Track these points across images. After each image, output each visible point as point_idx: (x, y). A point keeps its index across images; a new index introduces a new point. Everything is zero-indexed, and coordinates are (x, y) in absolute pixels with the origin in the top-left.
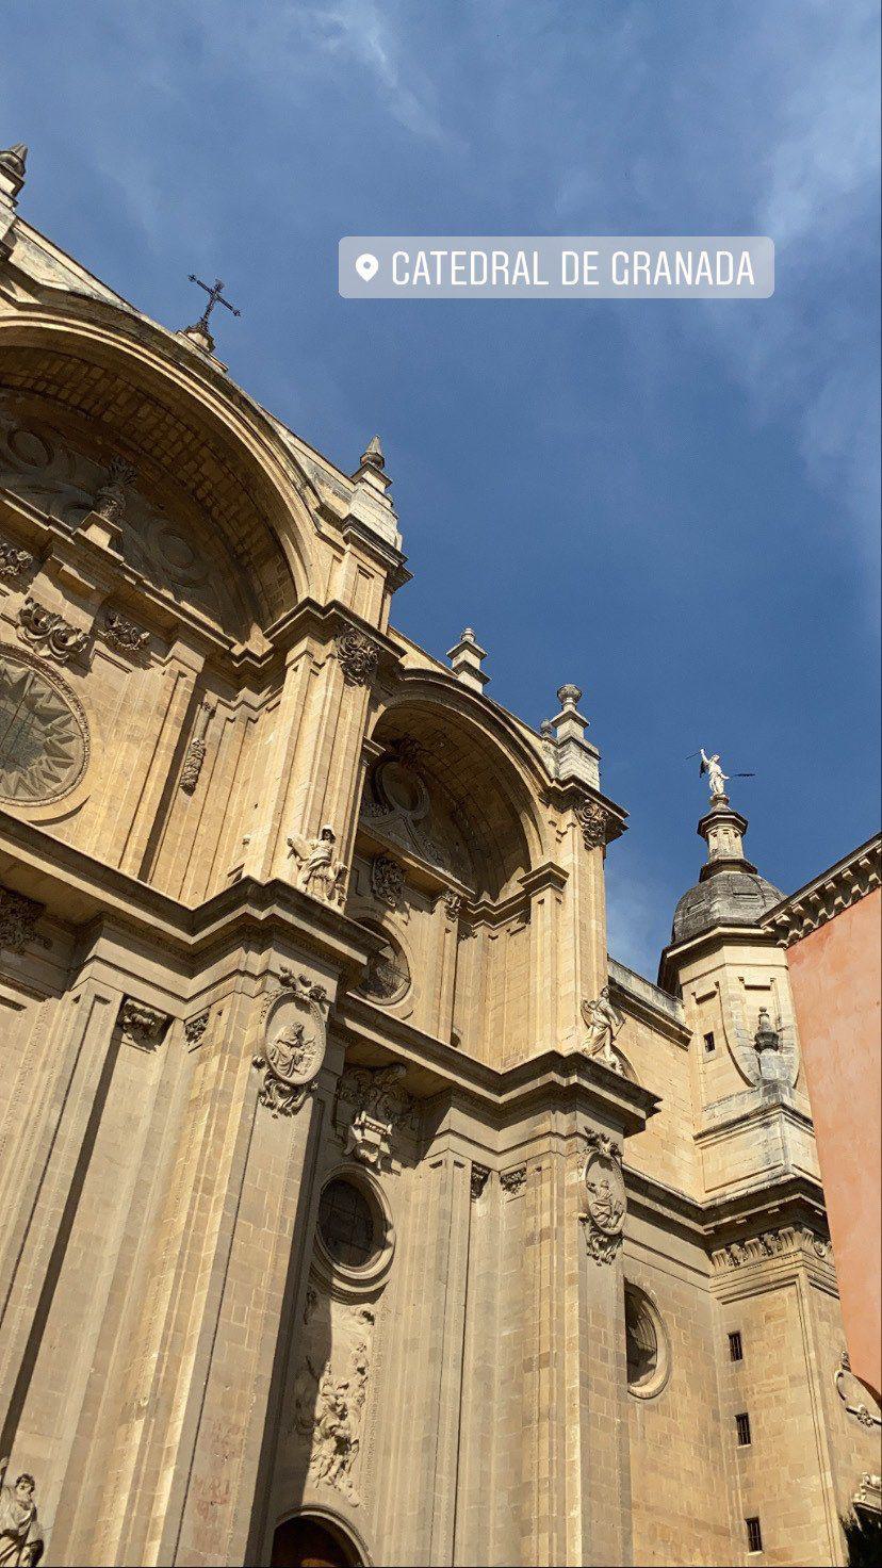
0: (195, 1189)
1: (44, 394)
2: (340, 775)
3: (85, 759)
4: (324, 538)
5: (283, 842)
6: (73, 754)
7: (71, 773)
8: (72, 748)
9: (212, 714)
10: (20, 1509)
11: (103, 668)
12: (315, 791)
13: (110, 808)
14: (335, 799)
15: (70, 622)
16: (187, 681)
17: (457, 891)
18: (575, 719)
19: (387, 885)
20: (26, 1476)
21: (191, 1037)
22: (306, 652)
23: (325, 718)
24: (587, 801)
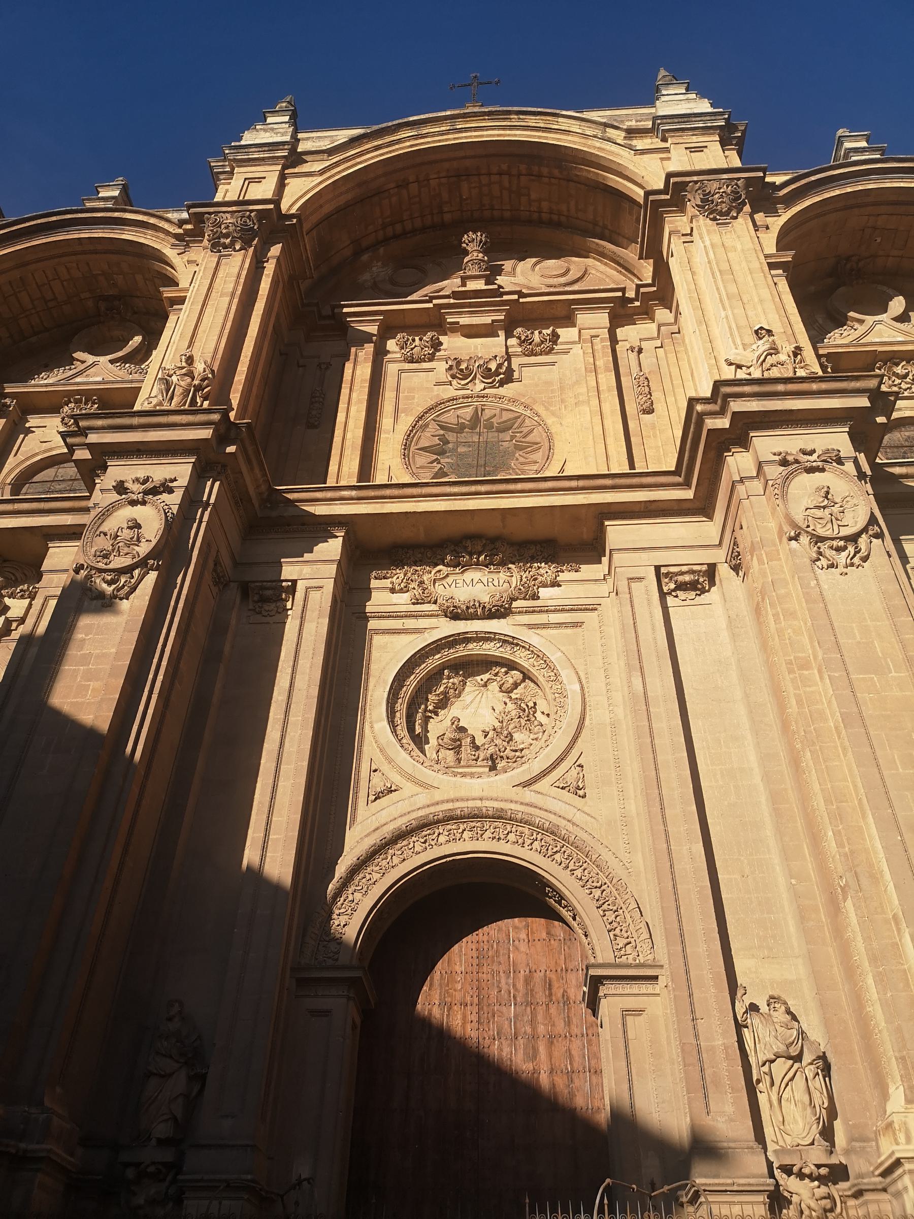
0: (791, 671)
1: (396, 237)
4: (643, 152)
6: (538, 440)
7: (543, 452)
10: (780, 1030)
12: (733, 314)
13: (586, 458)
14: (760, 309)
15: (487, 357)
19: (897, 381)
20: (772, 997)
21: (736, 568)
22: (670, 235)
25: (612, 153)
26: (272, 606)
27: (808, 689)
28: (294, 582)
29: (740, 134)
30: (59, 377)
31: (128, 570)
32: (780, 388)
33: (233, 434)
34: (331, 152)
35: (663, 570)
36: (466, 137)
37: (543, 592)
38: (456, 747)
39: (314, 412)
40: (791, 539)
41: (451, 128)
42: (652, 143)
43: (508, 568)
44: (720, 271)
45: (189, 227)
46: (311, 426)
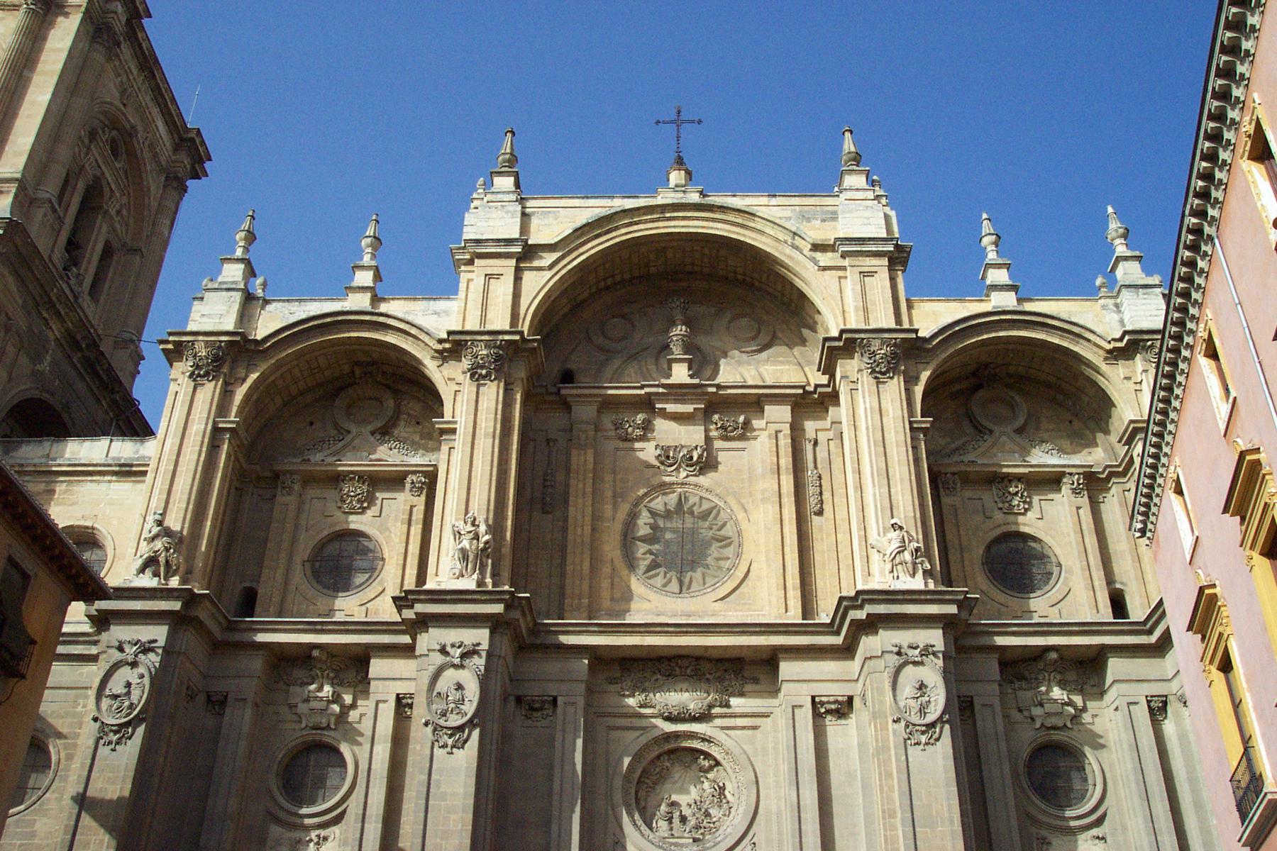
0: (884, 818)
1: (607, 288)
2: (897, 468)
3: (739, 533)
4: (825, 269)
5: (869, 547)
6: (731, 534)
8: (729, 531)
9: (816, 443)
11: (728, 455)
12: (880, 492)
14: (899, 488)
15: (689, 444)
16: (784, 434)
17: (1073, 470)
18: (1126, 258)
23: (870, 427)
24: (1149, 343)
25: (798, 263)
26: (539, 714)
27: (892, 833)
28: (555, 700)
29: (905, 255)
30: (329, 452)
31: (460, 728)
32: (900, 597)
33: (516, 604)
34: (556, 244)
35: (817, 699)
36: (674, 227)
37: (734, 701)
38: (670, 820)
39: (548, 499)
40: (894, 721)
41: (662, 216)
42: (832, 259)
43: (708, 679)
44: (874, 441)
45: (447, 346)
46: (545, 512)
